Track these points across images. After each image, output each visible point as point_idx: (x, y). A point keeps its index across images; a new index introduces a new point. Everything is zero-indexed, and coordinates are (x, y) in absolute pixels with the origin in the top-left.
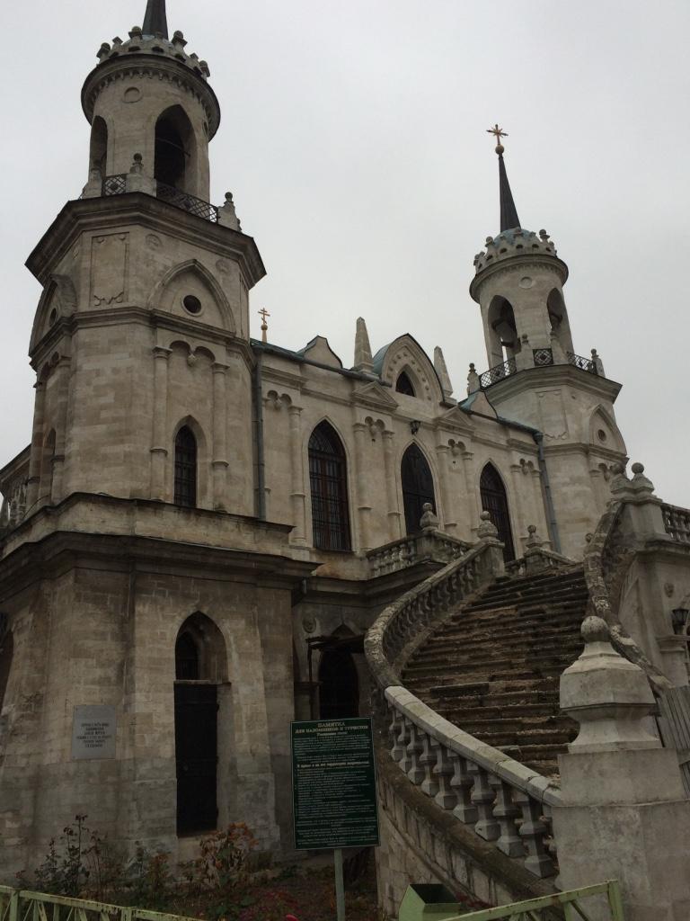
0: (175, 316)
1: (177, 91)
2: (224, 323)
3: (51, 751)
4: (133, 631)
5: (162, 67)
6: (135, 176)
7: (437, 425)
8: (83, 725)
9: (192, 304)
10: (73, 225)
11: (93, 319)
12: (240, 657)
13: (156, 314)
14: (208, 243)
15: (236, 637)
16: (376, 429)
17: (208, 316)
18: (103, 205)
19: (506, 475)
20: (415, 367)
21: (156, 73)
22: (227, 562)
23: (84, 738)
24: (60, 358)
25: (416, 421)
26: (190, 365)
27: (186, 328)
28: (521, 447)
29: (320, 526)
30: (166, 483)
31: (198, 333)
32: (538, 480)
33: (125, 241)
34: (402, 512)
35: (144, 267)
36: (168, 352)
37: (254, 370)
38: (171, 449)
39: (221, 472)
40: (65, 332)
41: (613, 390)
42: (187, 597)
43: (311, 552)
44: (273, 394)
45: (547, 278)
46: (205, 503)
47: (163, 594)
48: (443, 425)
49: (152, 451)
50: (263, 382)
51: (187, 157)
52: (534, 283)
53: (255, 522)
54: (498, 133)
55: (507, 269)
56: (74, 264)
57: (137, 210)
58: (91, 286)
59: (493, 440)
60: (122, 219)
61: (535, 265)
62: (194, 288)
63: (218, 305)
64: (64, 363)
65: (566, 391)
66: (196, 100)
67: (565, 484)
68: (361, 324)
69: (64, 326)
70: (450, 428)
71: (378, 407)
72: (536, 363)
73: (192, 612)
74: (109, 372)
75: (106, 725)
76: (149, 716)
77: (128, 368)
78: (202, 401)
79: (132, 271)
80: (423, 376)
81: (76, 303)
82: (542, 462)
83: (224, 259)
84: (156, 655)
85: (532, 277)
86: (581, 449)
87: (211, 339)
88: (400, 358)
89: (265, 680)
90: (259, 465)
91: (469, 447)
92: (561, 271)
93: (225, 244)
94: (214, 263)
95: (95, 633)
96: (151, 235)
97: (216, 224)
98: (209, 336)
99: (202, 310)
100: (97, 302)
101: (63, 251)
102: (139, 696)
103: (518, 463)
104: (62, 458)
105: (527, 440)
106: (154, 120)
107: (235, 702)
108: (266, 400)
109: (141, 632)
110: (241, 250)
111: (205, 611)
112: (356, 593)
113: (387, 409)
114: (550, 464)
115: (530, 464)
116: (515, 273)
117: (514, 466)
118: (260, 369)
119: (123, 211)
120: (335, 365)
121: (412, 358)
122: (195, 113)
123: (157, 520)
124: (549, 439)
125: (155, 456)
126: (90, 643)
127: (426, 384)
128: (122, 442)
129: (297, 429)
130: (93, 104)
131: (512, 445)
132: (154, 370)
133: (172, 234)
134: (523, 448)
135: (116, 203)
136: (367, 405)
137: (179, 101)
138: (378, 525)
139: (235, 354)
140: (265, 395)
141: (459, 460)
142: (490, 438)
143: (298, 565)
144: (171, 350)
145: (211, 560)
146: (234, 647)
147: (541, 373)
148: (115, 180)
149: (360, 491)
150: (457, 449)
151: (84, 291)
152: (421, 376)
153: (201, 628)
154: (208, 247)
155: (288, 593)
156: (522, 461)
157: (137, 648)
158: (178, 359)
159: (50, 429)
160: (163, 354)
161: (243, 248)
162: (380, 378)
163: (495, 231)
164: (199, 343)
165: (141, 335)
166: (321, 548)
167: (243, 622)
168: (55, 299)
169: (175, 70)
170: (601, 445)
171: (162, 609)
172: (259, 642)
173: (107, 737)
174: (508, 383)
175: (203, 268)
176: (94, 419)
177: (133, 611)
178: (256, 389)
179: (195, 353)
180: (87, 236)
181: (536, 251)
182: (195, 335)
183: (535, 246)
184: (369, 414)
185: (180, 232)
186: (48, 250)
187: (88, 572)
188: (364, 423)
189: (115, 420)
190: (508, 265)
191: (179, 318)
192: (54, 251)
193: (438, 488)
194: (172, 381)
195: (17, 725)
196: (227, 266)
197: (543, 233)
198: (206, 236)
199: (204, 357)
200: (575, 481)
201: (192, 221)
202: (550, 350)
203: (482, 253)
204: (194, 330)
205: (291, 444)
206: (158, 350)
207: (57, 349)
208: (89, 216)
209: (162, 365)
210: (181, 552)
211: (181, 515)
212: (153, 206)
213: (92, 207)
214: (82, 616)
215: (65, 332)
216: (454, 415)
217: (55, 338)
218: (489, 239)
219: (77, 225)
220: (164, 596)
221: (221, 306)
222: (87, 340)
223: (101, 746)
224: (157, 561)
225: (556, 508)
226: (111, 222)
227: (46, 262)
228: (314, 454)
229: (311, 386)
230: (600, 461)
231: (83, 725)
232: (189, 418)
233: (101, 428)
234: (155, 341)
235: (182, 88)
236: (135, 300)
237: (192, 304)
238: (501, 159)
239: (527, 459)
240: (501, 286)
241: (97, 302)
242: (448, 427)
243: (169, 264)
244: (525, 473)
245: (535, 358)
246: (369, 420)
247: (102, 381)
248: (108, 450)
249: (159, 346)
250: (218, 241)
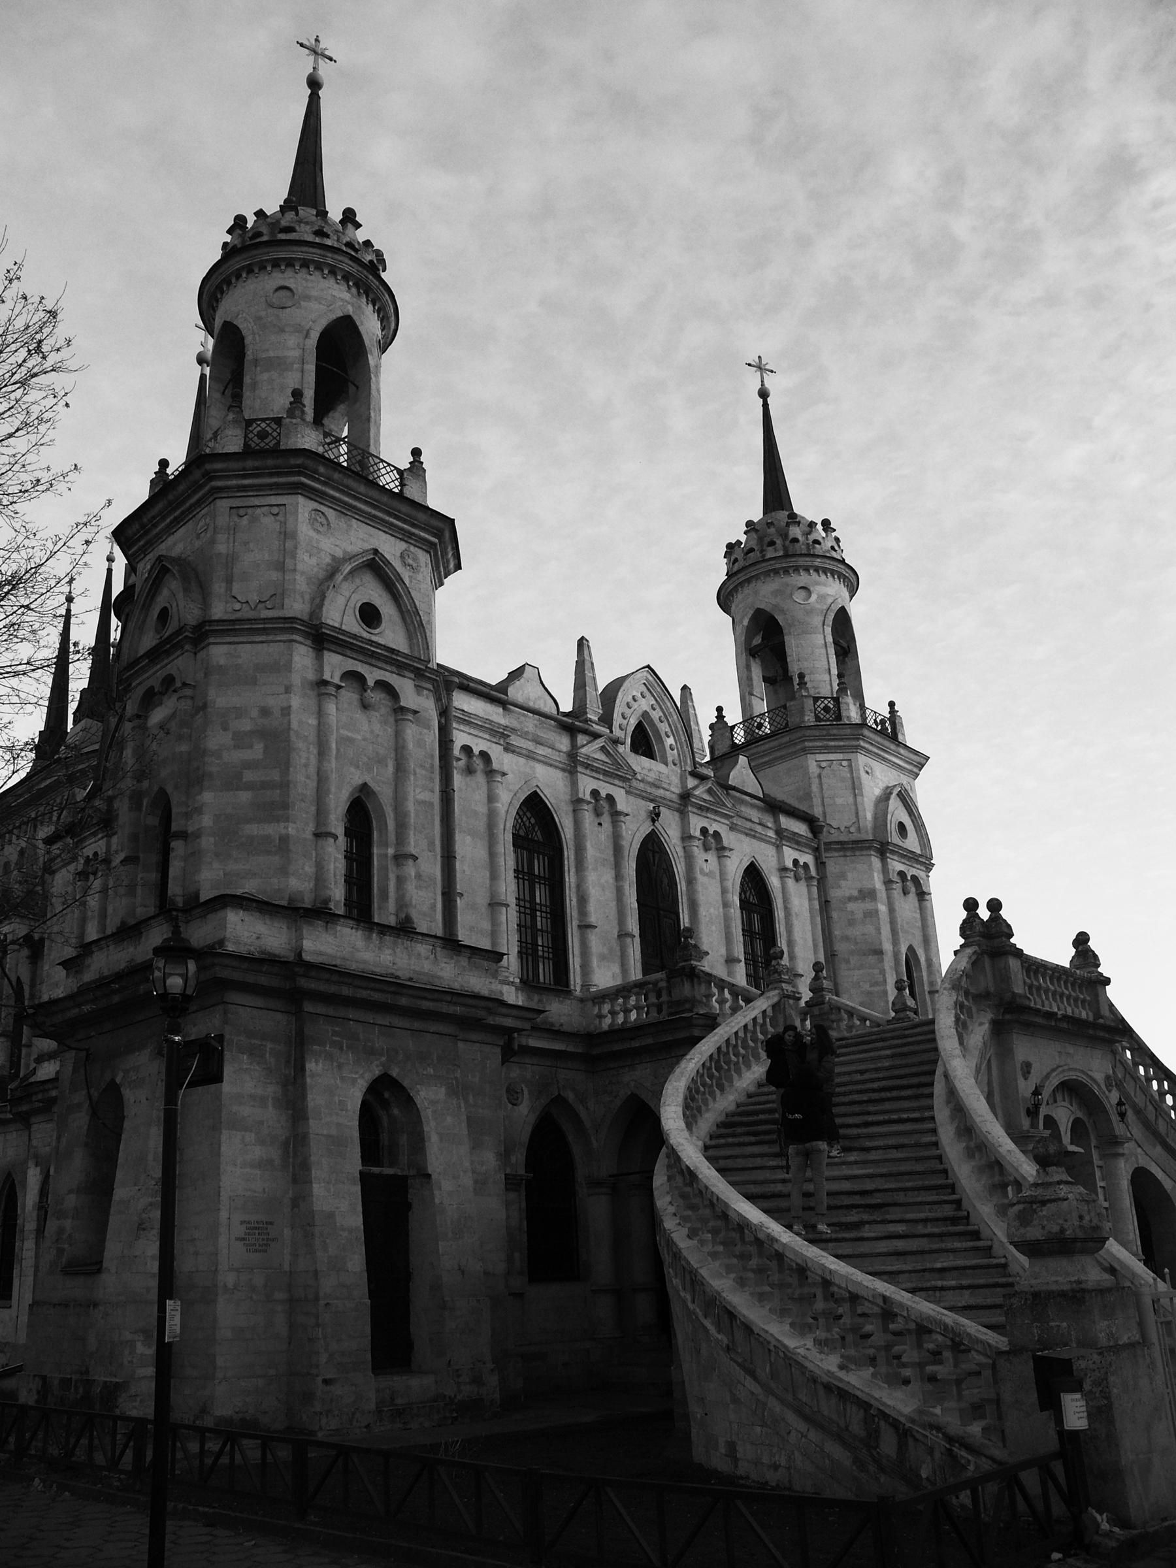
0: (344, 633)
1: (346, 296)
2: (411, 647)
3: (196, 1254)
4: (303, 1097)
5: (329, 261)
6: (294, 421)
8: (242, 1223)
10: (201, 487)
11: (234, 628)
12: (441, 1141)
13: (324, 631)
14: (392, 524)
15: (434, 1112)
16: (605, 806)
17: (391, 634)
18: (250, 463)
19: (774, 881)
20: (656, 715)
21: (319, 267)
22: (426, 1005)
23: (244, 1239)
24: (178, 684)
26: (365, 706)
27: (362, 651)
29: (527, 952)
31: (379, 659)
32: (815, 890)
33: (279, 518)
34: (636, 932)
35: (306, 558)
36: (339, 687)
37: (444, 712)
38: (340, 830)
40: (187, 647)
41: (919, 761)
42: (371, 1052)
43: (517, 989)
44: (467, 749)
45: (833, 589)
46: (386, 914)
50: (455, 732)
51: (352, 389)
52: (814, 597)
53: (450, 943)
54: (760, 368)
55: (776, 572)
56: (197, 544)
57: (299, 474)
58: (229, 581)
60: (277, 485)
63: (404, 619)
64: (188, 692)
68: (582, 643)
69: (186, 636)
70: (703, 809)
72: (817, 718)
73: (377, 1073)
74: (255, 713)
75: (271, 1223)
76: (331, 1216)
77: (283, 709)
78: (381, 761)
79: (289, 563)
80: (668, 729)
81: (206, 605)
82: (820, 864)
83: (412, 548)
84: (334, 1132)
85: (812, 589)
87: (394, 669)
89: (474, 1172)
91: (728, 838)
92: (851, 581)
93: (414, 525)
94: (398, 554)
95: (253, 1097)
96: (316, 510)
97: (400, 496)
98: (391, 664)
99: (383, 625)
100: (237, 606)
101: (177, 522)
102: (317, 1189)
103: (789, 864)
104: (183, 835)
105: (800, 828)
106: (315, 336)
107: (437, 1201)
109: (315, 1099)
110: (435, 535)
111: (394, 1073)
112: (579, 1051)
113: (620, 778)
114: (834, 865)
115: (806, 865)
116: (787, 579)
119: (279, 474)
120: (550, 708)
122: (370, 326)
123: (330, 939)
124: (833, 831)
125: (321, 842)
126: (246, 1111)
128: (277, 820)
129: (499, 805)
130: (217, 301)
133: (346, 510)
134: (798, 843)
135: (270, 462)
136: (593, 770)
137: (350, 310)
138: (605, 951)
139: (425, 692)
140: (456, 751)
141: (712, 857)
143: (515, 1012)
144: (343, 684)
145: (403, 1001)
146: (433, 1124)
147: (825, 732)
148: (263, 425)
149: (583, 900)
150: (714, 843)
151: (218, 587)
152: (663, 728)
153: (386, 1095)
154: (391, 530)
155: (498, 1050)
156: (796, 862)
157: (311, 1121)
158: (349, 696)
159: (156, 788)
160: (332, 690)
161: (439, 534)
162: (611, 731)
163: (756, 513)
165: (302, 657)
166: (528, 983)
167: (443, 1089)
168: (165, 592)
169: (348, 266)
170: (901, 844)
171: (340, 1067)
172: (464, 1117)
173: (272, 1240)
174: (775, 743)
175: (387, 563)
176: (233, 782)
177: (301, 1069)
179: (373, 689)
180: (223, 505)
182: (373, 661)
183: (816, 542)
185: (354, 507)
186: (154, 517)
187: (241, 1009)
188: (588, 797)
189: (265, 785)
190: (778, 566)
191: (355, 637)
192: (163, 519)
193: (685, 898)
194: (342, 731)
195: (144, 1216)
196: (415, 559)
197: (826, 524)
198: (389, 514)
199: (383, 695)
201: (375, 494)
202: (836, 700)
203: (739, 543)
204: (373, 655)
205: (491, 826)
206: (325, 683)
207: (171, 669)
208: (228, 477)
210: (366, 988)
211: (360, 933)
212: (322, 469)
213: (233, 465)
214: (235, 1072)
215: (187, 647)
217: (168, 653)
218: (749, 524)
219: (207, 488)
220: (341, 1049)
221: (409, 621)
222: (222, 662)
223: (266, 1251)
226: (260, 487)
227: (146, 533)
228: (520, 842)
231: (242, 1223)
232: (365, 786)
233: (245, 796)
234: (320, 669)
235: (354, 290)
236: (297, 607)
237: (370, 615)
238: (766, 406)
240: (764, 594)
241: (237, 606)
242: (700, 808)
243: (339, 554)
244: (797, 879)
245: (815, 709)
246: (595, 793)
247: (246, 725)
248: (252, 829)
249: (327, 677)
250: (405, 521)
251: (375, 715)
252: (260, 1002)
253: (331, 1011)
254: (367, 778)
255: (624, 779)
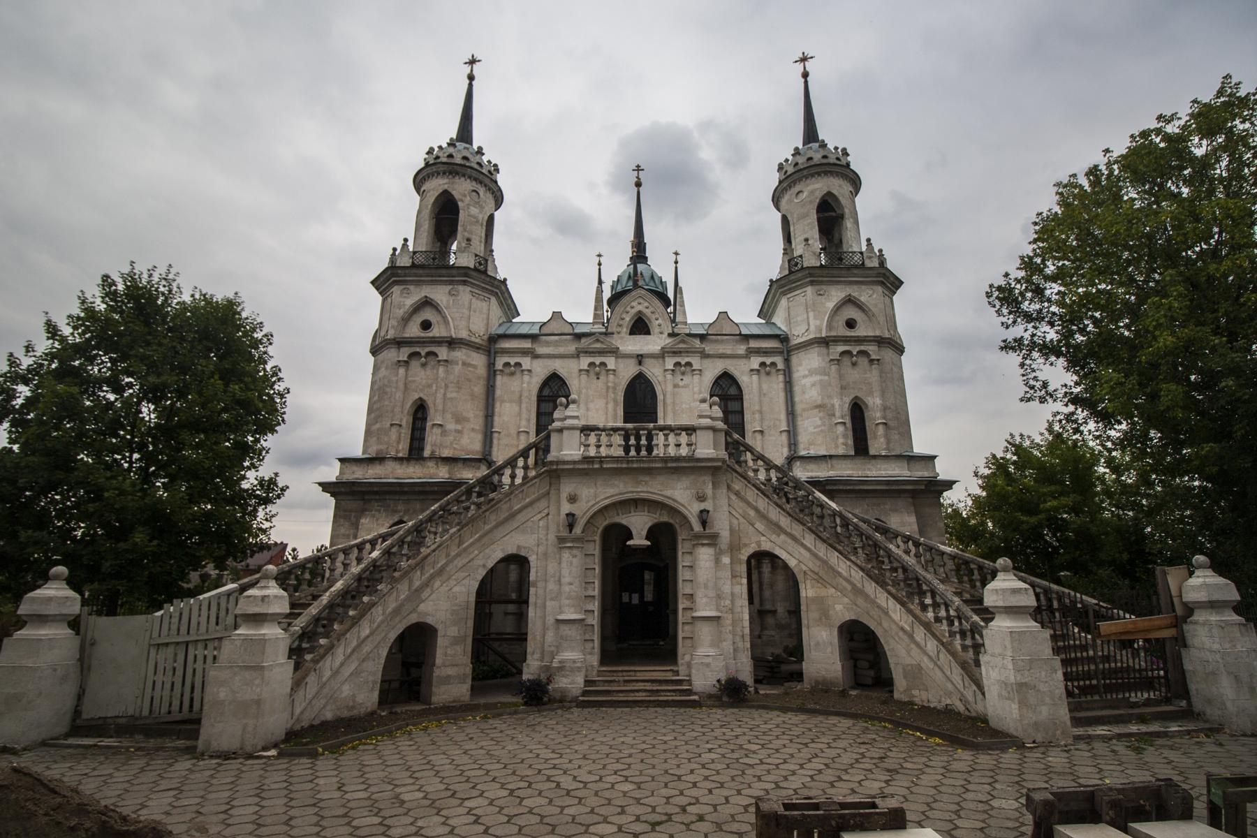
7: (662, 354)
9: (426, 325)
16: (596, 370)
19: (745, 380)
20: (647, 312)
25: (641, 355)
26: (424, 365)
28: (766, 352)
30: (398, 443)
39: (437, 431)
42: (395, 512)
44: (507, 365)
46: (427, 453)
47: (379, 511)
48: (668, 352)
49: (392, 425)
52: (805, 194)
59: (729, 352)
61: (806, 177)
62: (428, 314)
65: (809, 290)
66: (463, 179)
67: (805, 377)
71: (601, 353)
86: (818, 343)
88: (632, 307)
90: (489, 417)
94: (447, 291)
95: (344, 535)
103: (756, 366)
108: (501, 371)
113: (610, 352)
114: (794, 360)
115: (773, 364)
116: (793, 190)
117: (752, 370)
118: (493, 351)
120: (568, 330)
121: (646, 304)
127: (657, 322)
131: (751, 352)
132: (397, 375)
137: (446, 187)
142: (724, 351)
145: (406, 489)
152: (654, 317)
158: (415, 364)
164: (427, 350)
170: (853, 334)
178: (491, 366)
181: (811, 163)
184: (591, 360)
200: (812, 372)
204: (424, 342)
206: (399, 361)
209: (402, 371)
216: (683, 342)
224: (376, 493)
225: (797, 399)
229: (541, 350)
230: (841, 348)
237: (426, 325)
238: (806, 83)
239: (768, 361)
242: (674, 352)
251: (429, 367)
252: (350, 498)
253: (377, 497)
254: (422, 395)
255: (613, 352)
